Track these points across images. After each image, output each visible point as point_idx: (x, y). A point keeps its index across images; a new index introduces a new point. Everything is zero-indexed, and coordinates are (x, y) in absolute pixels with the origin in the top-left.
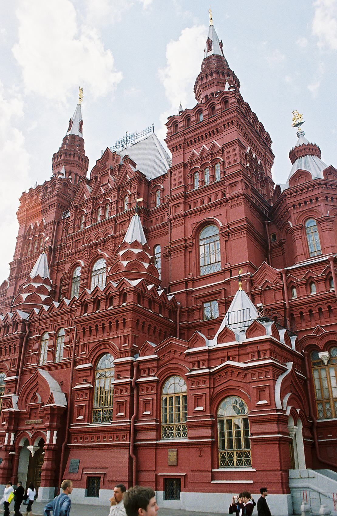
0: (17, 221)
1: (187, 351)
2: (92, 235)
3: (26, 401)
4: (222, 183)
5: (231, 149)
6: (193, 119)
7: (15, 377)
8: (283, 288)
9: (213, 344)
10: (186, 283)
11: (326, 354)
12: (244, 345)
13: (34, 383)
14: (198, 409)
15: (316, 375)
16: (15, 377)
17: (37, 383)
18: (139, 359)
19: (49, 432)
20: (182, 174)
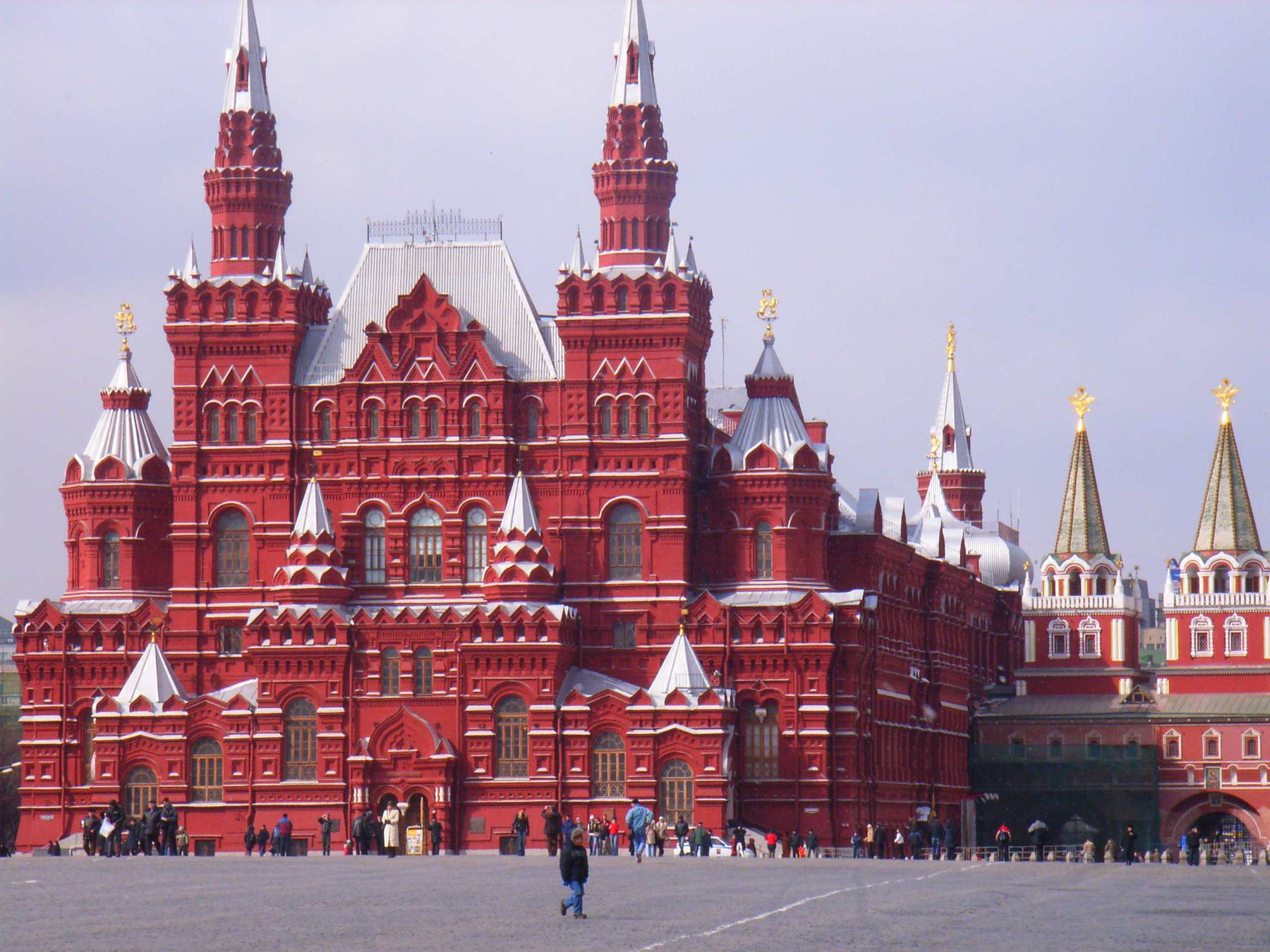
1: (628, 708)
2: (413, 459)
3: (382, 745)
4: (655, 445)
5: (671, 390)
6: (610, 300)
7: (341, 710)
8: (725, 630)
9: (661, 705)
10: (590, 587)
11: (764, 711)
12: (695, 712)
13: (397, 725)
14: (639, 769)
15: (748, 731)
16: (341, 710)
17: (402, 725)
18: (564, 708)
19: (441, 789)
20: (584, 399)
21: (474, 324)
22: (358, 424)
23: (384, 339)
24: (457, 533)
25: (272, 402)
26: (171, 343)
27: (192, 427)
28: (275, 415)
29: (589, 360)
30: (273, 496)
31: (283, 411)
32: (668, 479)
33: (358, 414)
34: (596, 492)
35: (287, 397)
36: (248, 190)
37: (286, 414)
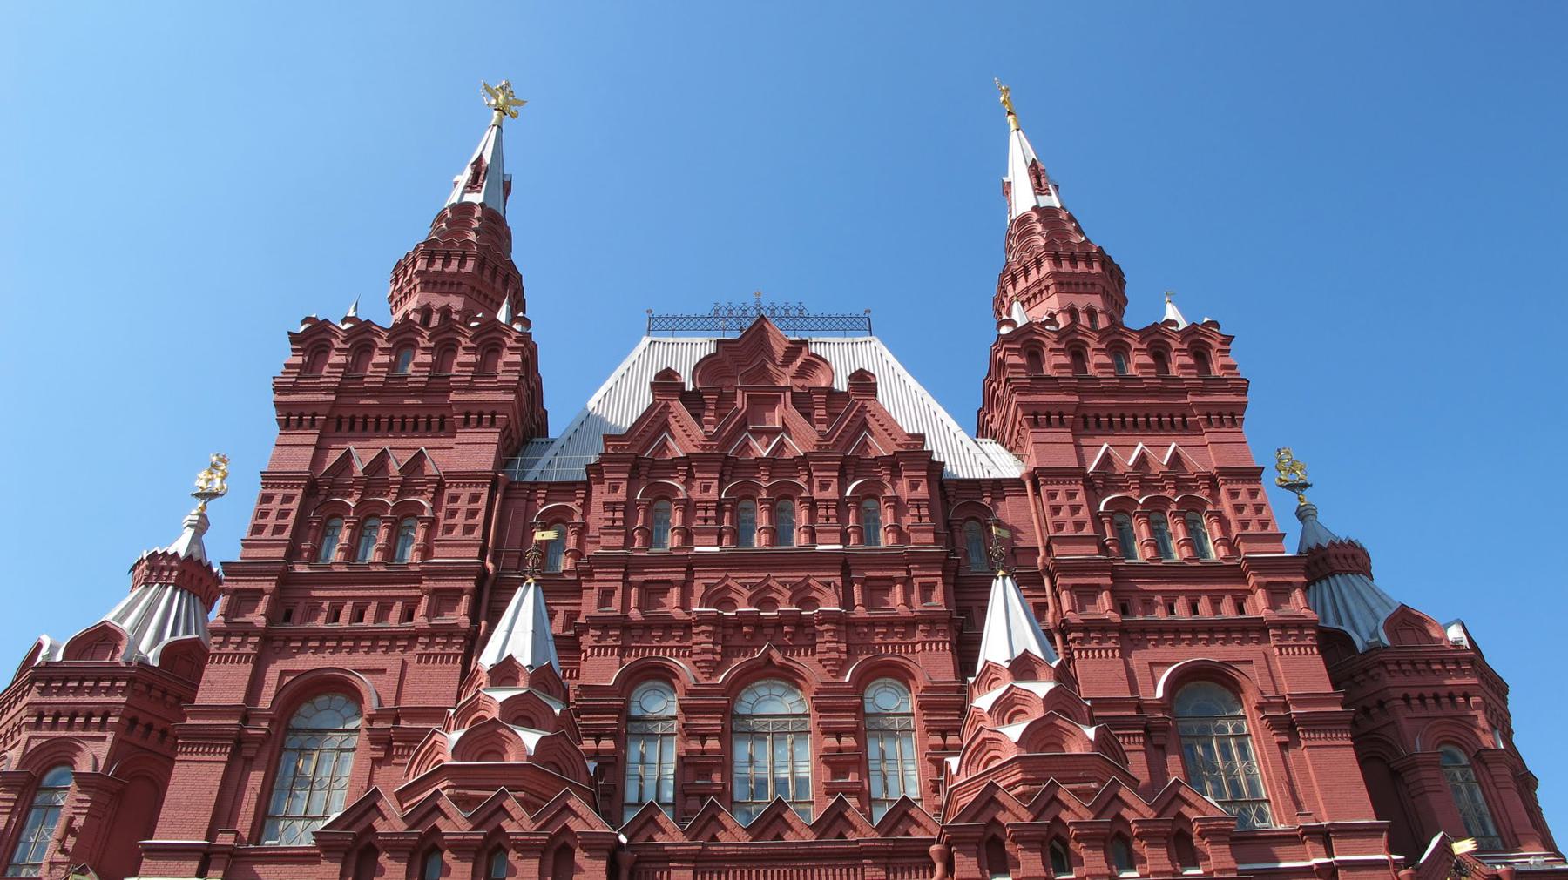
0: (272, 413)
21: (863, 381)
22: (629, 519)
23: (685, 397)
24: (848, 720)
25: (454, 498)
26: (277, 405)
27: (286, 535)
28: (460, 519)
29: (1078, 446)
30: (424, 658)
31: (472, 514)
32: (1283, 625)
33: (629, 508)
34: (1139, 659)
35: (486, 491)
36: (462, 263)
37: (480, 519)
